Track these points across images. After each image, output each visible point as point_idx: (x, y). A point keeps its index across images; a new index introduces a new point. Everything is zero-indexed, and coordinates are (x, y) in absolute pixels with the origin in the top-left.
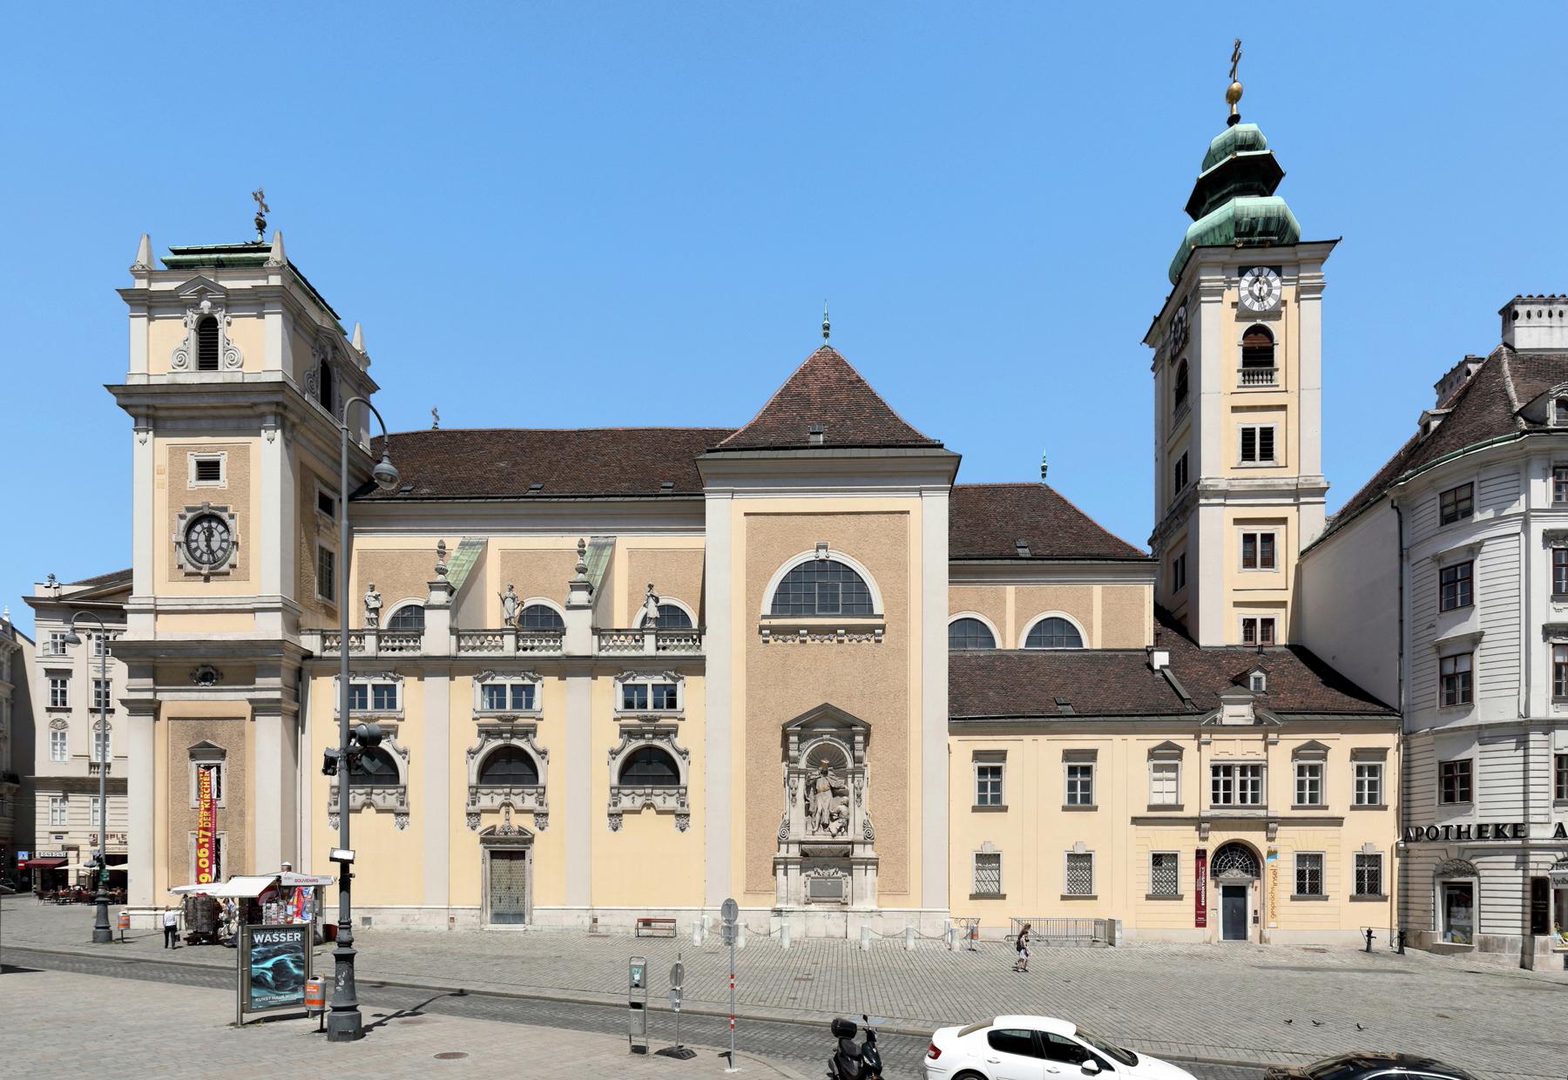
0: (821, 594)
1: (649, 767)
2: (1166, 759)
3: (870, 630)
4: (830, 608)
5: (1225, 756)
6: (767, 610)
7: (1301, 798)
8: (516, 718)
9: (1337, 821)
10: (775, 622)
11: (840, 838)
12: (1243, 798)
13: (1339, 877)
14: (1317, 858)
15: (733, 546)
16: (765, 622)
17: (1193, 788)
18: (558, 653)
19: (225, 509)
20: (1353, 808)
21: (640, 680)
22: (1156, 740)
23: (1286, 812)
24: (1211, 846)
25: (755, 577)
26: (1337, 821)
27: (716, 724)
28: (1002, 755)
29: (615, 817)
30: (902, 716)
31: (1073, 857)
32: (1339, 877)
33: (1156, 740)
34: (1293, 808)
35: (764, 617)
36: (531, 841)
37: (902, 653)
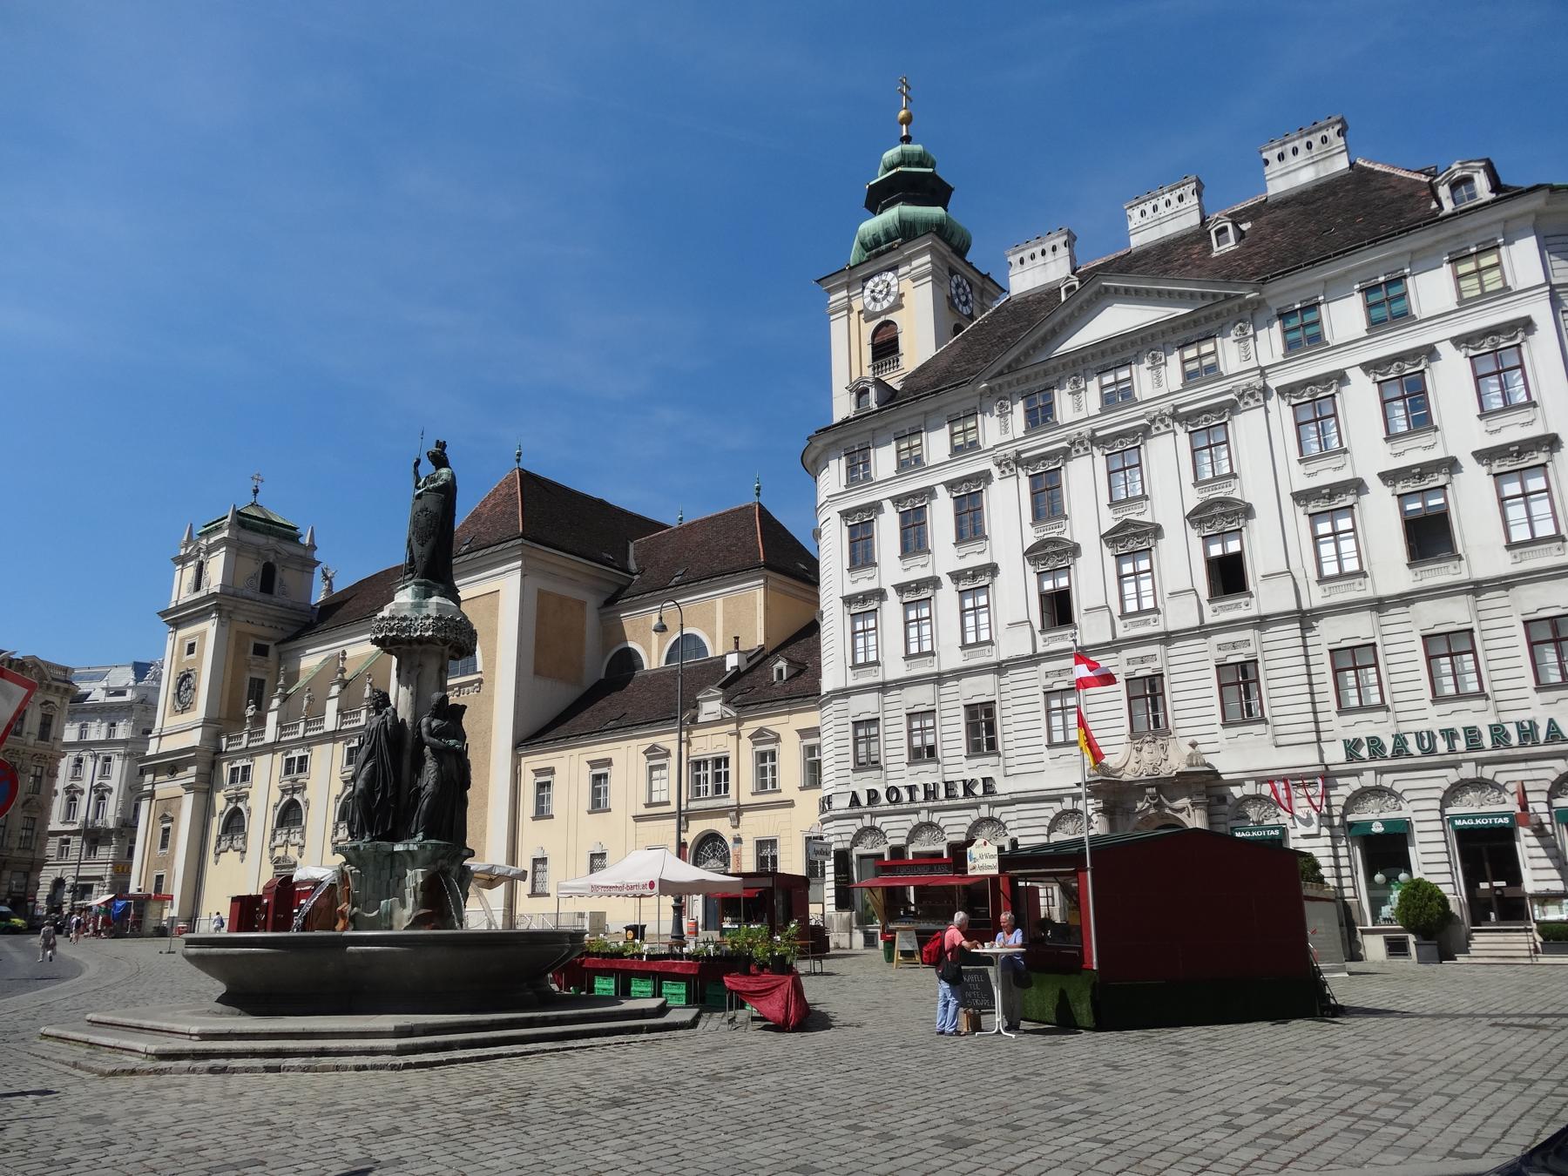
3: (470, 683)
5: (720, 749)
7: (764, 784)
9: (790, 804)
12: (718, 790)
14: (773, 843)
23: (746, 799)
24: (689, 838)
26: (790, 804)
28: (551, 771)
31: (593, 856)
36: (295, 865)
37: (491, 698)
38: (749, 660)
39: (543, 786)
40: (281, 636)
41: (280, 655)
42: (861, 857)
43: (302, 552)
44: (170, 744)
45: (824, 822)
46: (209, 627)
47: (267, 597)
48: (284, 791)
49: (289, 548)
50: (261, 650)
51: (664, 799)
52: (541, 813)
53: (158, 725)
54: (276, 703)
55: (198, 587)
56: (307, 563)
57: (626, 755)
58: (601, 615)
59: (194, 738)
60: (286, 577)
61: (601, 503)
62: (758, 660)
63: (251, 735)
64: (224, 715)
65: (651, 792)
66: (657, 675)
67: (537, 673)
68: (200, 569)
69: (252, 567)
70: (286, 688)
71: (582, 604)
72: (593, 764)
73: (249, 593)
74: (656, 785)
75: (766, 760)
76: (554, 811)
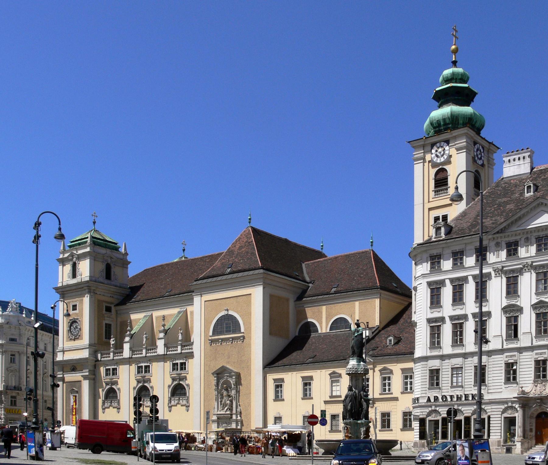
0: (227, 325)
1: (178, 391)
2: (335, 378)
3: (238, 338)
4: (228, 331)
6: (211, 334)
8: (145, 376)
9: (396, 399)
10: (213, 338)
11: (227, 413)
13: (397, 421)
14: (388, 415)
15: (200, 312)
16: (210, 338)
17: (343, 388)
18: (155, 354)
19: (77, 319)
20: (402, 393)
21: (177, 362)
22: (331, 371)
23: (377, 396)
25: (207, 323)
26: (396, 399)
27: (196, 375)
29: (170, 407)
30: (249, 368)
32: (397, 421)
33: (331, 371)
34: (380, 394)
35: (210, 336)
37: (250, 345)
38: (373, 333)
39: (277, 387)
40: (117, 302)
41: (116, 311)
42: (430, 421)
43: (121, 257)
44: (69, 356)
45: (414, 408)
46: (86, 300)
47: (109, 281)
48: (139, 382)
49: (115, 254)
50: (108, 309)
51: (338, 394)
52: (278, 398)
53: (61, 345)
54: (127, 339)
55: (74, 276)
56: (125, 263)
57: (321, 377)
58: (295, 305)
59: (85, 354)
60: (116, 270)
61: (286, 241)
62: (377, 332)
63: (114, 353)
64: (96, 342)
65: (332, 391)
66: (326, 335)
67: (271, 334)
68: (74, 266)
69: (102, 267)
70: (130, 331)
71: (288, 300)
72: (303, 378)
73: (101, 280)
74: (334, 388)
75: (386, 380)
76: (284, 397)
